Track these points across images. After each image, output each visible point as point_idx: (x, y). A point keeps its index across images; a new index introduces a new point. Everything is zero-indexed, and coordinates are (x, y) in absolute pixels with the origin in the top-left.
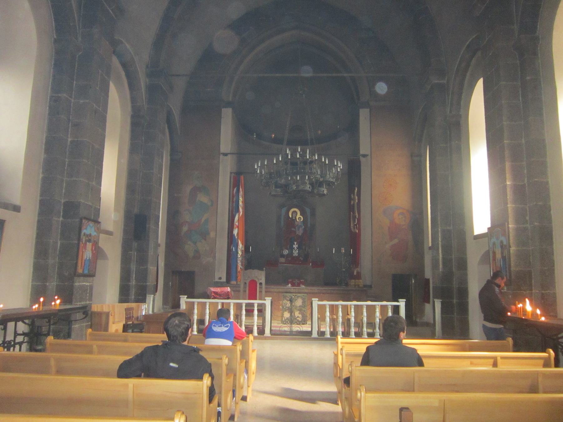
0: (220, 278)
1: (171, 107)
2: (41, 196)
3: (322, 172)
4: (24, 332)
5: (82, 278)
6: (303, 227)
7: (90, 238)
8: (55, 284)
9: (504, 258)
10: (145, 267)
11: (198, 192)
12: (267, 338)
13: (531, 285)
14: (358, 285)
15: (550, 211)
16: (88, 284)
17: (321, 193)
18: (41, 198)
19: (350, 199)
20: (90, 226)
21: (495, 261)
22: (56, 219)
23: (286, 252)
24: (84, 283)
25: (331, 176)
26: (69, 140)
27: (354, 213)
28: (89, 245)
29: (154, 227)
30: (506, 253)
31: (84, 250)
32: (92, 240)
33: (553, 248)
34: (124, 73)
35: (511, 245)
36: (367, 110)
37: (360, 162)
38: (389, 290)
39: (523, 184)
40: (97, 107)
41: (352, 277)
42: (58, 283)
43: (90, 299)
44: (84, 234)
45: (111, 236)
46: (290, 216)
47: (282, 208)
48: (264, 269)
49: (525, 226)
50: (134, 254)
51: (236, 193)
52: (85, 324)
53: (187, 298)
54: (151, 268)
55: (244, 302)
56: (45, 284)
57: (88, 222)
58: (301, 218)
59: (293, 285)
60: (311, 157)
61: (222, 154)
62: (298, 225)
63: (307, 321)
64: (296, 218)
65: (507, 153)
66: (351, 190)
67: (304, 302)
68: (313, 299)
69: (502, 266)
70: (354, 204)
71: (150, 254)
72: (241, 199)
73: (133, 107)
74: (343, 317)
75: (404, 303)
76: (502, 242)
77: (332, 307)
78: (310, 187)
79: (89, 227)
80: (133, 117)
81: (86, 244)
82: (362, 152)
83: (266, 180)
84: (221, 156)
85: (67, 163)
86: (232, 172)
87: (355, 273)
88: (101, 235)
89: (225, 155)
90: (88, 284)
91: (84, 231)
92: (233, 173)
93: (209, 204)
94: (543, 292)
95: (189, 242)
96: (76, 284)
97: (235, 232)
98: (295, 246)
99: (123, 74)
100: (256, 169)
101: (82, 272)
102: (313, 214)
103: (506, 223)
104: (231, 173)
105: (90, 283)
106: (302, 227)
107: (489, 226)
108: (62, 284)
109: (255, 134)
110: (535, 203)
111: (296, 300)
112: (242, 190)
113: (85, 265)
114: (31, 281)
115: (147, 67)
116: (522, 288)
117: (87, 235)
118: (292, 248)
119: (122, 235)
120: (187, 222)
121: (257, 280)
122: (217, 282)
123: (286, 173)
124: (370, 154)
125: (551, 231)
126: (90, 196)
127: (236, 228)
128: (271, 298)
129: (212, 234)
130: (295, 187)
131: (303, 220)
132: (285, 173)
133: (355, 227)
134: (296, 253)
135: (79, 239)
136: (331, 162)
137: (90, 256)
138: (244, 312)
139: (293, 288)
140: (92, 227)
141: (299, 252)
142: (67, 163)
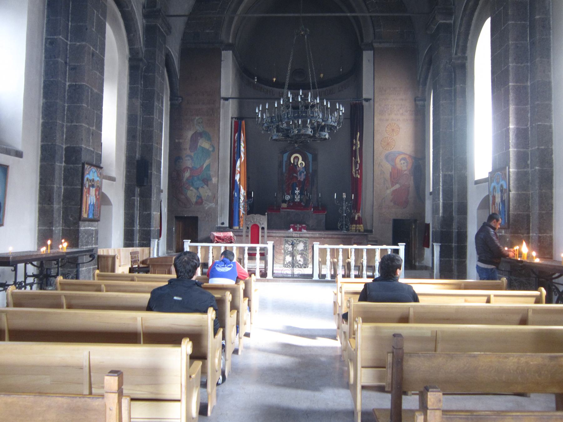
0: (223, 224)
1: (170, 49)
2: (42, 141)
3: (323, 115)
4: (34, 273)
5: (87, 223)
6: (305, 172)
7: (93, 183)
8: (61, 228)
9: (503, 201)
10: (149, 212)
11: (199, 138)
12: (268, 281)
13: (528, 229)
14: (359, 230)
15: (552, 154)
16: (94, 228)
17: (323, 137)
18: (42, 143)
19: (352, 145)
20: (93, 172)
21: (495, 205)
22: (58, 164)
23: (288, 197)
24: (90, 228)
25: (333, 120)
26: (68, 84)
27: (356, 158)
28: (93, 191)
29: (156, 173)
30: (506, 196)
31: (88, 195)
32: (95, 185)
33: (552, 193)
34: (120, 14)
35: (511, 188)
36: (371, 53)
37: (363, 106)
38: (390, 234)
39: (526, 127)
40: (94, 50)
41: (353, 221)
42: (63, 228)
43: (96, 243)
44: (87, 179)
45: (114, 182)
46: (292, 162)
47: (283, 154)
48: (266, 213)
49: (525, 170)
50: (137, 199)
51: (237, 138)
52: (92, 267)
53: (191, 242)
54: (154, 213)
55: (247, 246)
56: (51, 228)
57: (90, 167)
59: (295, 229)
60: (312, 100)
61: (223, 98)
62: (299, 171)
64: (297, 163)
65: (511, 96)
66: (353, 136)
67: (305, 246)
68: (314, 243)
69: (501, 209)
70: (356, 150)
71: (152, 199)
72: (242, 144)
73: (131, 50)
74: (344, 261)
75: (404, 246)
76: (502, 186)
77: (332, 250)
78: (311, 132)
79: (91, 173)
80: (130, 60)
81: (89, 189)
82: (364, 96)
83: (267, 124)
84: (222, 101)
85: (66, 108)
86: (234, 117)
87: (356, 218)
88: (104, 181)
89: (226, 99)
90: (94, 228)
91: (87, 177)
92: (234, 118)
93: (211, 149)
94: (540, 235)
95: (191, 188)
96: (82, 228)
97: (237, 178)
98: (297, 192)
99: (119, 14)
100: (257, 113)
101: (86, 217)
102: (315, 159)
103: (507, 168)
104: (232, 118)
105: (95, 227)
106: (303, 172)
107: (491, 170)
108: (68, 228)
109: (256, 78)
110: (537, 147)
111: (298, 244)
112: (243, 135)
113: (89, 210)
114: (37, 226)
115: (144, 7)
116: (520, 231)
117: (90, 180)
118: (294, 194)
119: (124, 181)
120: (189, 168)
121: (259, 225)
122: (220, 228)
124: (372, 98)
125: (552, 175)
126: (91, 140)
127: (237, 174)
128: (273, 242)
129: (214, 180)
130: (297, 132)
132: (286, 117)
133: (357, 172)
134: (297, 199)
135: (82, 184)
136: (333, 105)
137: (95, 201)
138: (246, 256)
139: (295, 233)
140: (95, 172)
141: (300, 198)
142: (66, 108)
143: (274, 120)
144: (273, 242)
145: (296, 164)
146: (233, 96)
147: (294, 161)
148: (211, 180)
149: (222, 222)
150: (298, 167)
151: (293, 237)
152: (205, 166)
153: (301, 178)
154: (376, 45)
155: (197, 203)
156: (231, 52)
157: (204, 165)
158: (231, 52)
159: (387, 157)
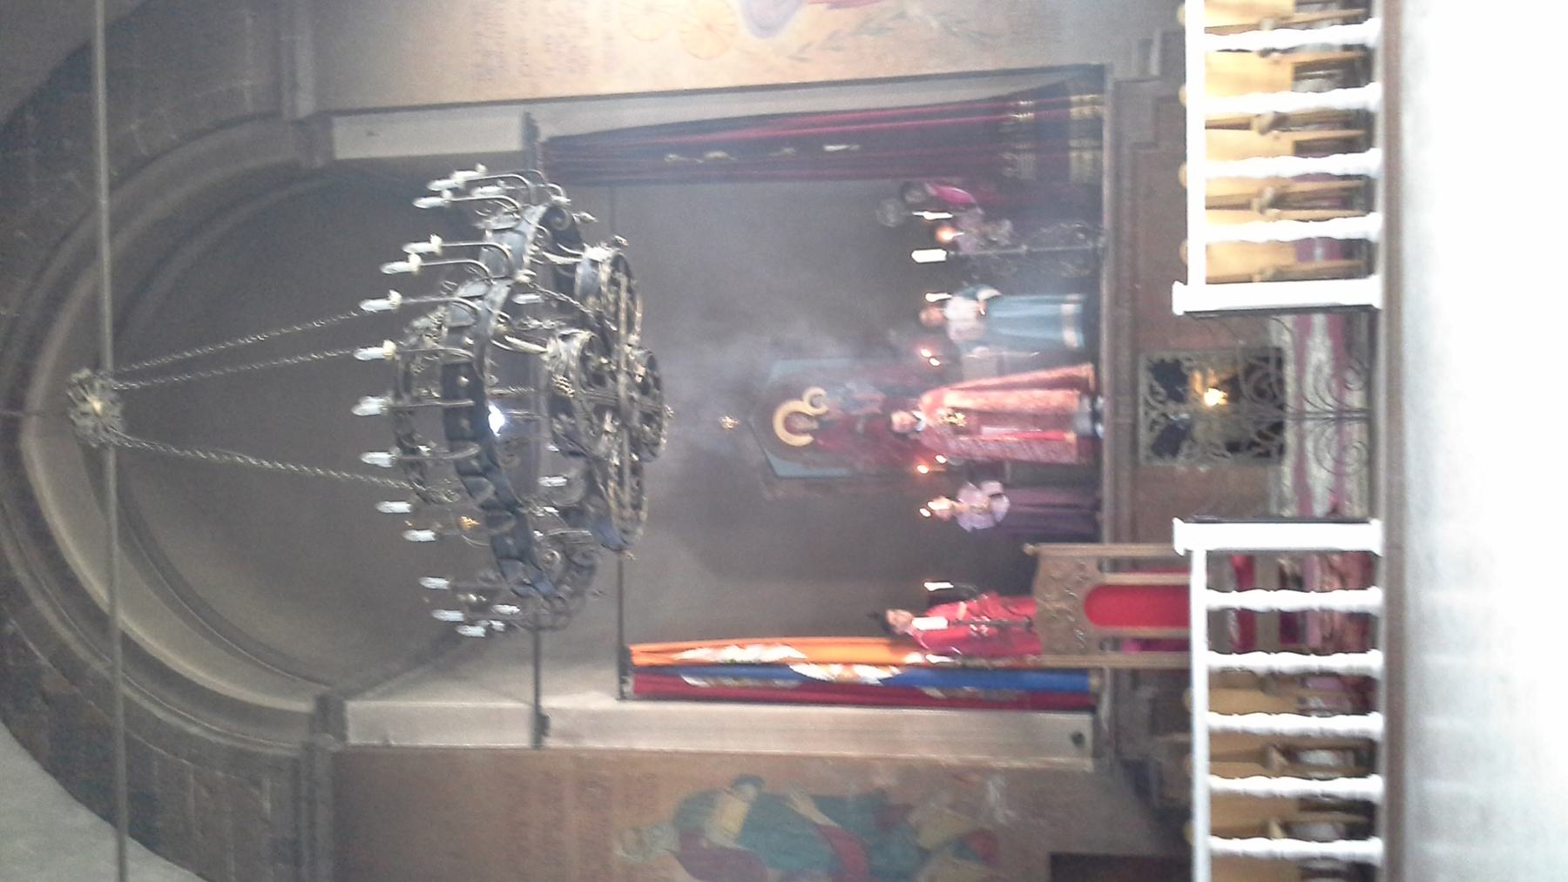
12: (1395, 542)
46: (805, 440)
47: (777, 476)
55: (1204, 660)
58: (816, 396)
63: (1265, 348)
72: (733, 653)
78: (564, 338)
84: (551, 742)
86: (617, 694)
89: (541, 723)
93: (750, 791)
97: (872, 675)
104: (623, 697)
106: (850, 391)
123: (485, 472)
124: (522, 108)
128: (1177, 521)
131: (822, 387)
138: (1258, 661)
143: (510, 541)
144: (1177, 521)
145: (815, 425)
146: (530, 697)
147: (804, 432)
148: (882, 793)
149: (1070, 744)
150: (827, 413)
151: (1134, 427)
152: (821, 819)
153: (872, 401)
154: (305, 105)
155: (988, 858)
156: (353, 706)
157: (819, 822)
158: (353, 706)
159: (765, 28)
